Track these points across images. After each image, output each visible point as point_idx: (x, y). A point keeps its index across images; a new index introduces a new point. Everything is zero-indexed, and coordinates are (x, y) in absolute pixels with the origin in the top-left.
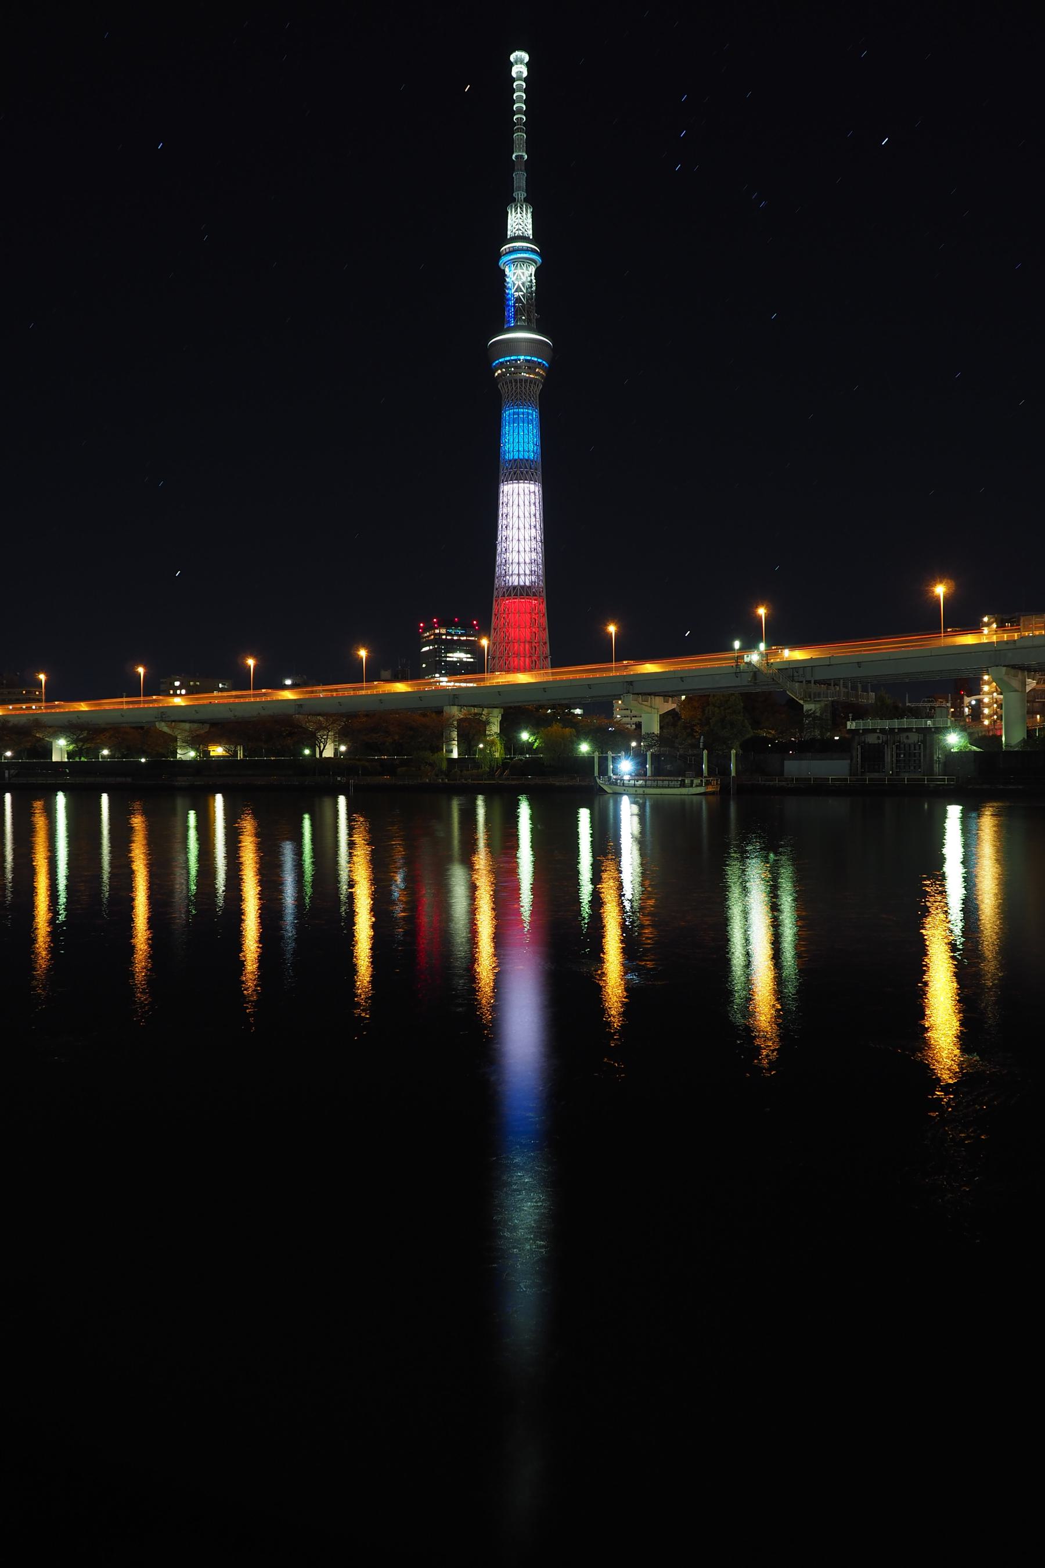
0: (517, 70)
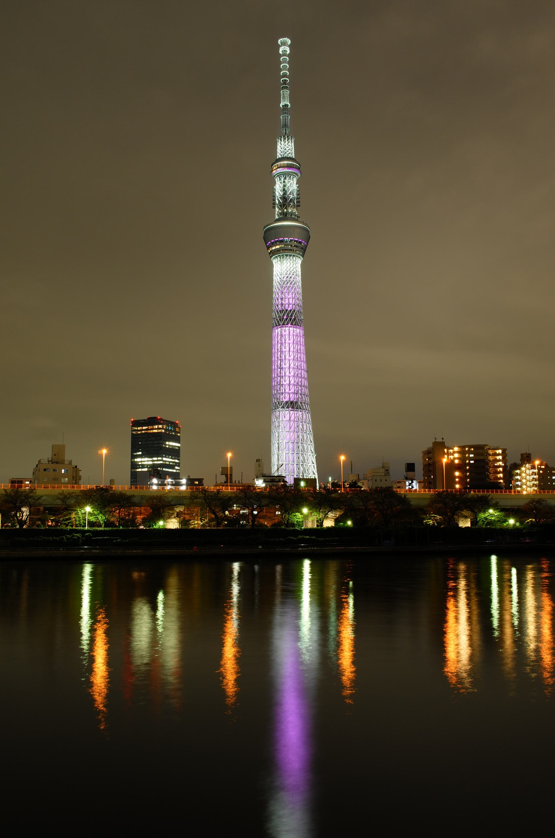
0: (283, 49)
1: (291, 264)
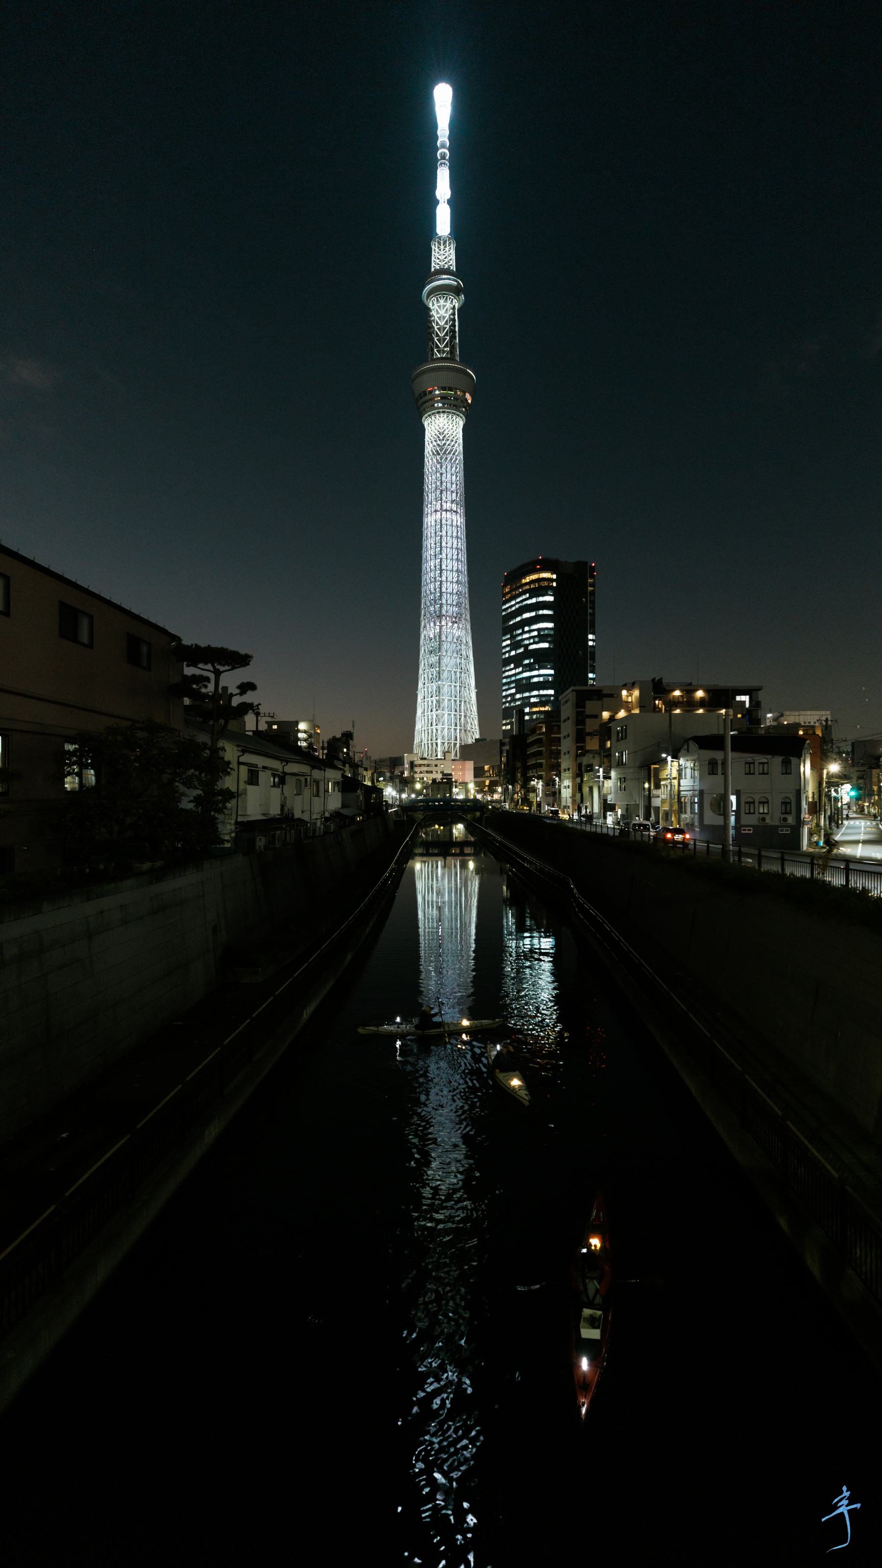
1: (453, 426)
